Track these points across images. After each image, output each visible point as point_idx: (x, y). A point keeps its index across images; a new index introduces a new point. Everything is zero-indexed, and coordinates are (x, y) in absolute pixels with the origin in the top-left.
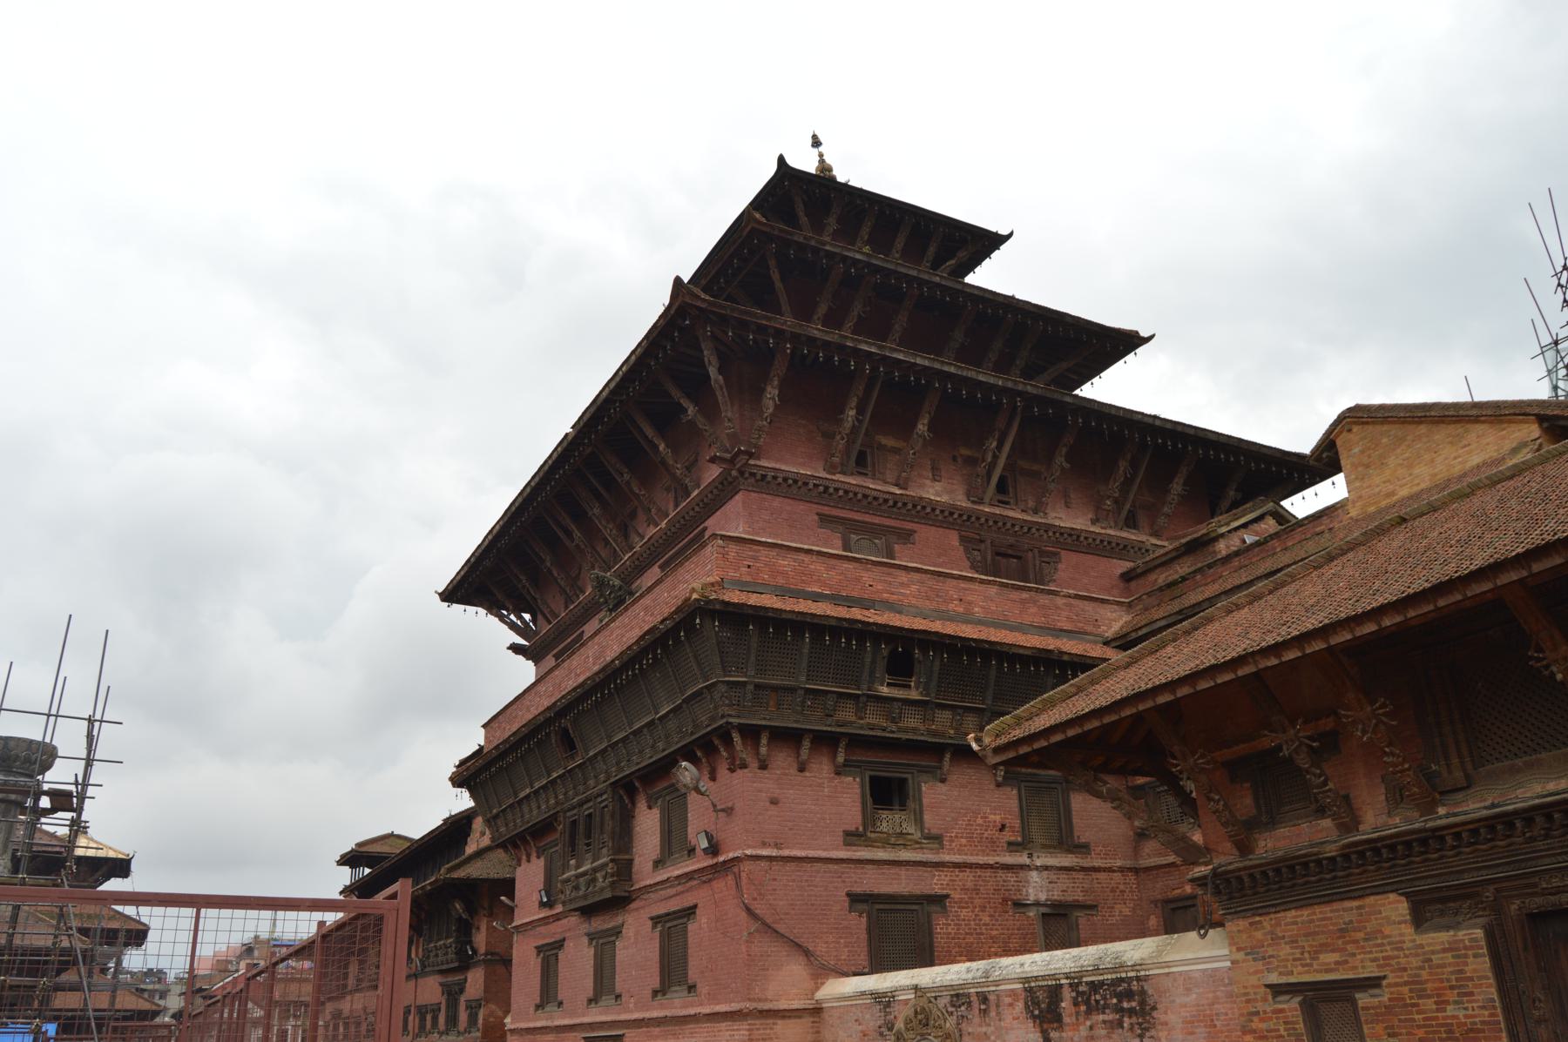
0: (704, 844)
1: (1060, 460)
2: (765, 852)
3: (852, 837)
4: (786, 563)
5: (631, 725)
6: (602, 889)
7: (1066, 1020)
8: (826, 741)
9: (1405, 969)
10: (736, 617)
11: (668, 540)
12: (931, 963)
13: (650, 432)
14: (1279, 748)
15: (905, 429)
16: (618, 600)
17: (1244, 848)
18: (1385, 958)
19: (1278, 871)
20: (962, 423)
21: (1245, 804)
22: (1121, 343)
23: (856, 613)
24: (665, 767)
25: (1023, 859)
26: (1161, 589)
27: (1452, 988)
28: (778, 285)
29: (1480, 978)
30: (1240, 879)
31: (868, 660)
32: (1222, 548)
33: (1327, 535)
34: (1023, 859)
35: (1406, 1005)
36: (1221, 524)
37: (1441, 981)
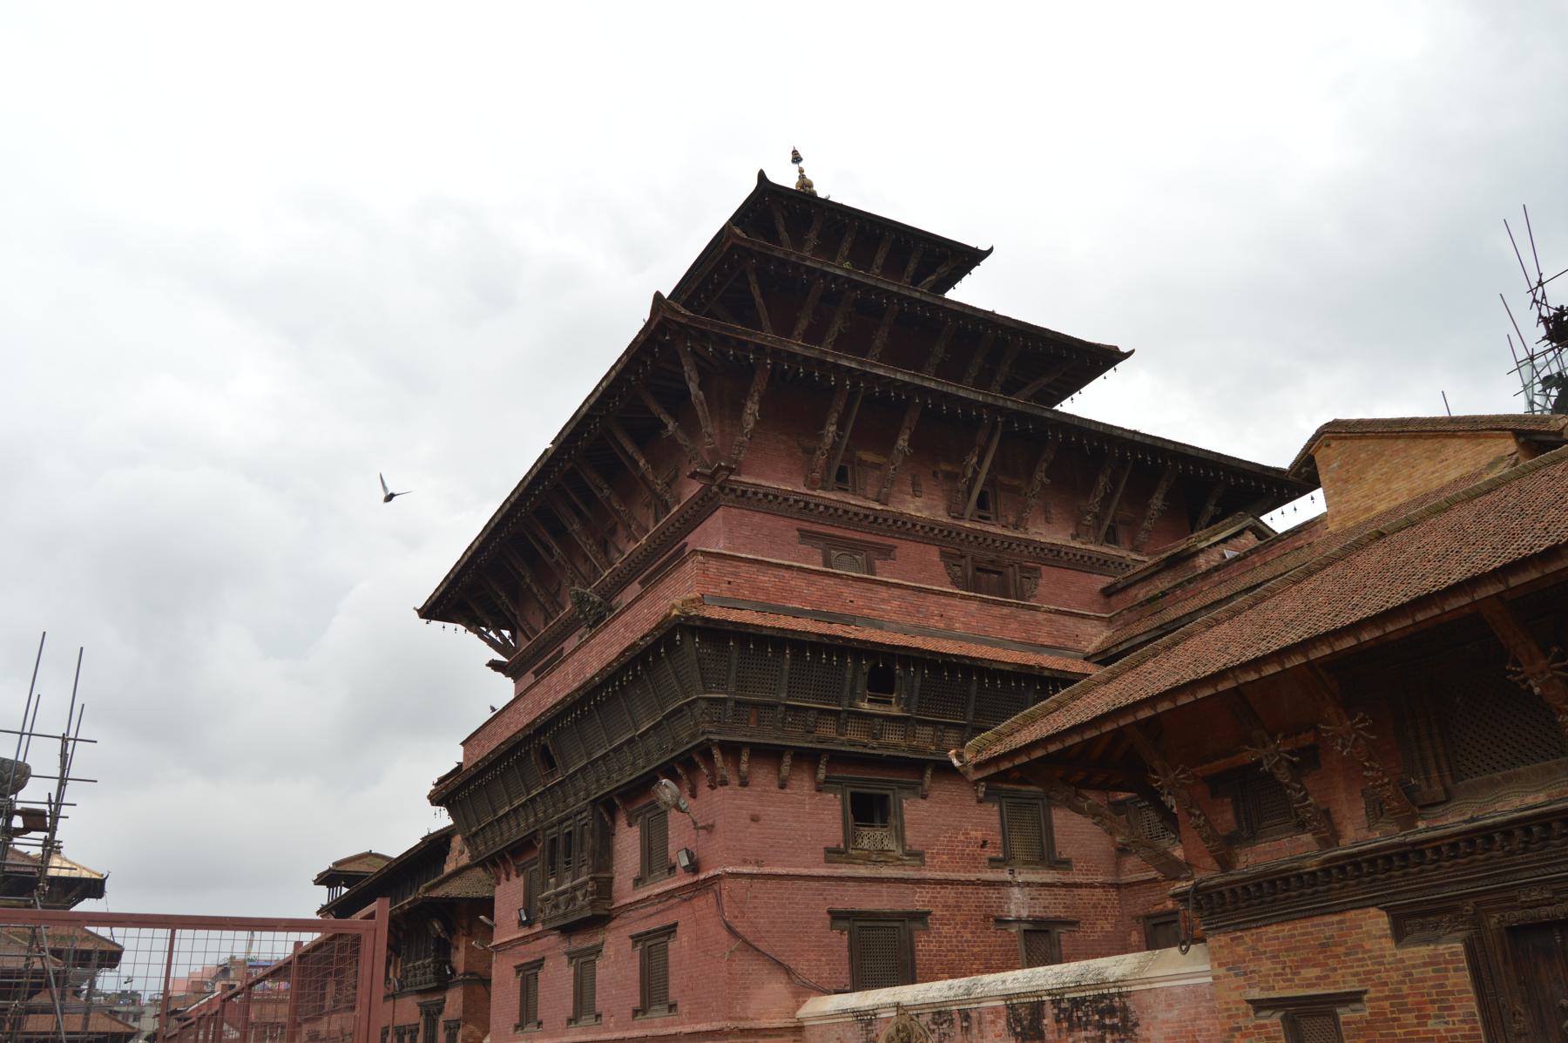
0: (685, 862)
1: (1040, 476)
2: (746, 870)
3: (833, 854)
4: (766, 579)
5: (610, 742)
6: (582, 908)
8: (806, 758)
9: (1386, 984)
10: (715, 633)
11: (649, 555)
12: (914, 982)
14: (1259, 763)
15: (885, 444)
16: (598, 616)
17: (1225, 864)
18: (1366, 973)
19: (1259, 886)
20: (942, 439)
21: (1226, 819)
22: (1100, 359)
23: (837, 629)
24: (646, 784)
25: (1005, 875)
26: (1141, 604)
27: (1433, 1002)
28: (759, 300)
29: (1460, 992)
30: (1221, 894)
31: (849, 676)
32: (1202, 563)
34: (1005, 875)
35: (1387, 1020)
37: (1422, 995)
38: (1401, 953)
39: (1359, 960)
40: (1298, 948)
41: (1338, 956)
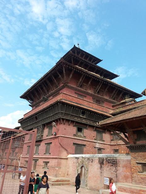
0: (55, 134)
1: (106, 90)
2: (63, 136)
3: (75, 135)
4: (70, 98)
5: (50, 115)
6: (38, 139)
7: (104, 164)
8: (73, 122)
10: (63, 103)
11: (54, 93)
12: (83, 154)
13: (54, 78)
14: (143, 130)
15: (87, 83)
16: (45, 100)
19: (140, 147)
20: (95, 82)
21: (136, 137)
22: (116, 76)
23: (79, 105)
24: (51, 123)
28: (73, 62)
30: (134, 147)
31: (79, 112)
32: (127, 104)
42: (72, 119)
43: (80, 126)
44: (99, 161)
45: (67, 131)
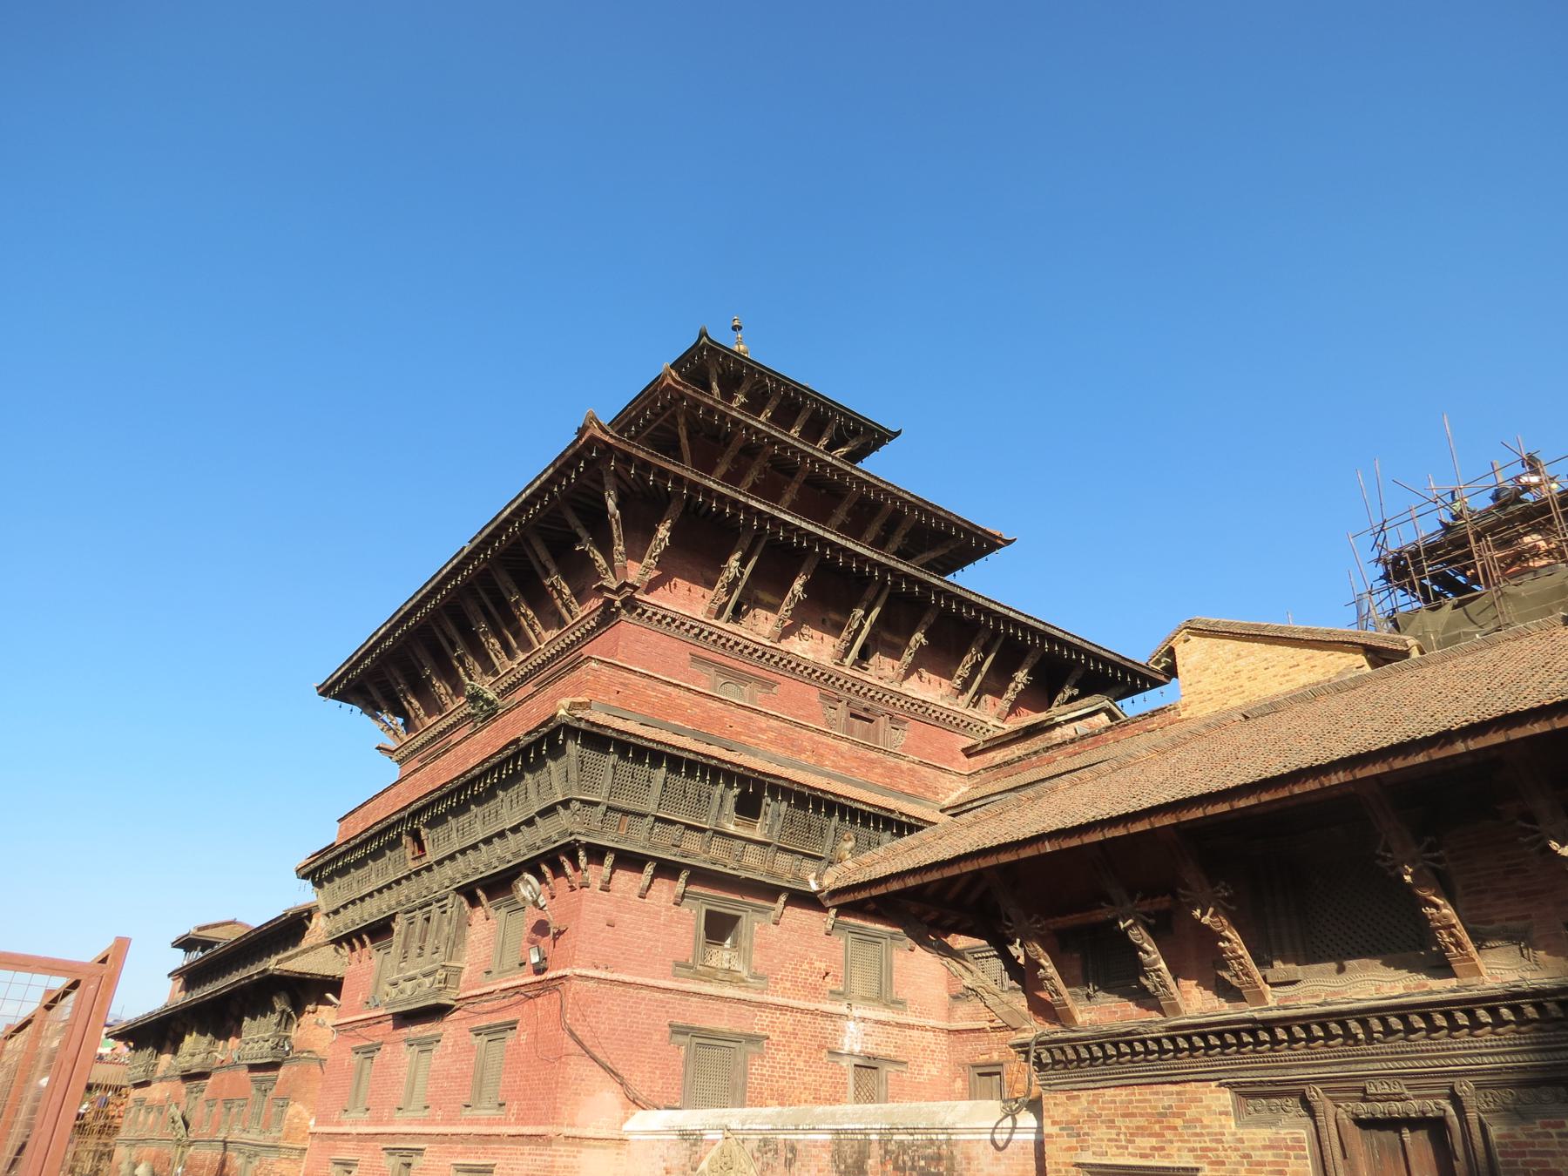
4: (655, 693)
6: (426, 995)
9: (1223, 1163)
10: (597, 739)
12: (742, 1105)
13: (544, 555)
18: (1202, 1149)
26: (998, 766)
28: (684, 441)
32: (1057, 734)
33: (1158, 732)
34: (843, 1009)
36: (1058, 712)
38: (1244, 1133)
39: (1197, 1135)
40: (1133, 1115)
41: (1175, 1128)
42: (666, 849)
43: (725, 902)
44: (837, 1155)
45: (628, 929)
